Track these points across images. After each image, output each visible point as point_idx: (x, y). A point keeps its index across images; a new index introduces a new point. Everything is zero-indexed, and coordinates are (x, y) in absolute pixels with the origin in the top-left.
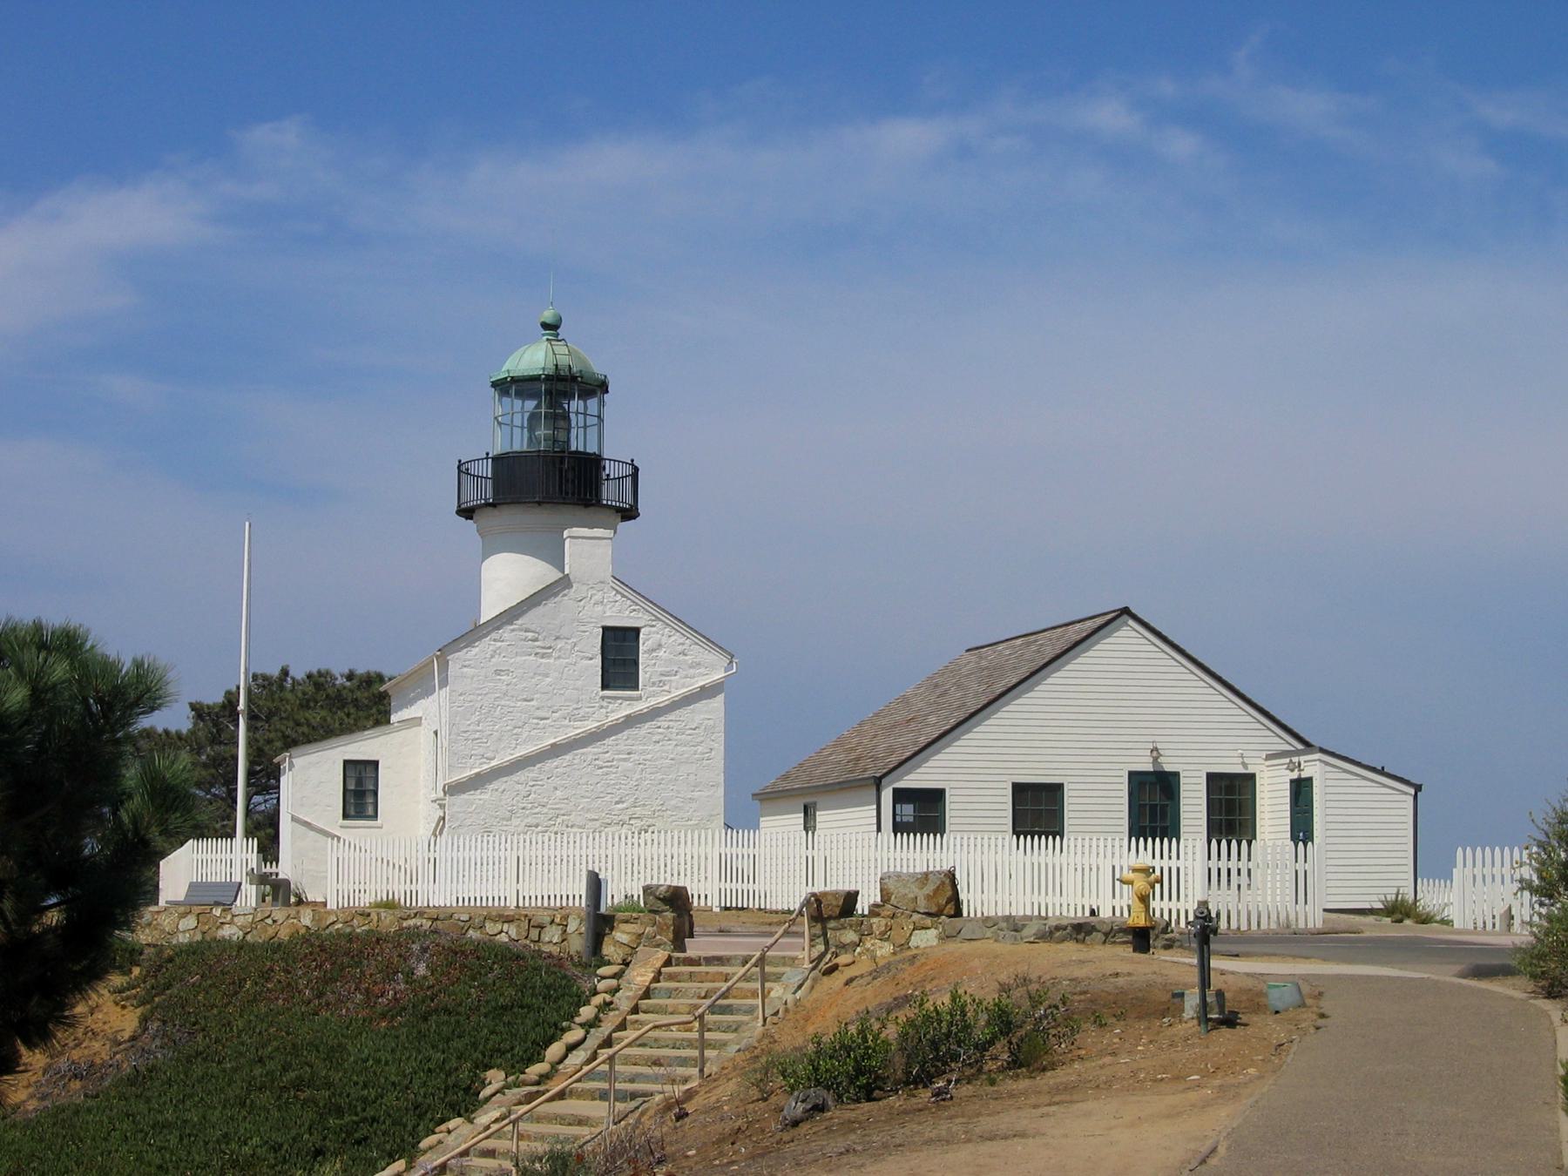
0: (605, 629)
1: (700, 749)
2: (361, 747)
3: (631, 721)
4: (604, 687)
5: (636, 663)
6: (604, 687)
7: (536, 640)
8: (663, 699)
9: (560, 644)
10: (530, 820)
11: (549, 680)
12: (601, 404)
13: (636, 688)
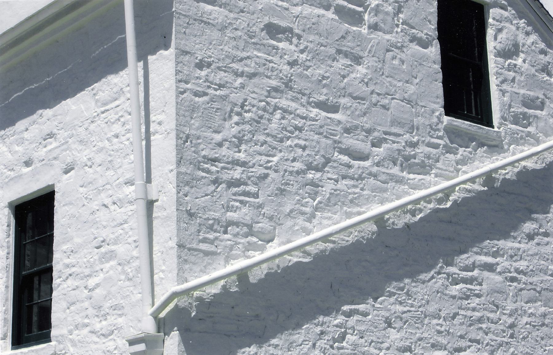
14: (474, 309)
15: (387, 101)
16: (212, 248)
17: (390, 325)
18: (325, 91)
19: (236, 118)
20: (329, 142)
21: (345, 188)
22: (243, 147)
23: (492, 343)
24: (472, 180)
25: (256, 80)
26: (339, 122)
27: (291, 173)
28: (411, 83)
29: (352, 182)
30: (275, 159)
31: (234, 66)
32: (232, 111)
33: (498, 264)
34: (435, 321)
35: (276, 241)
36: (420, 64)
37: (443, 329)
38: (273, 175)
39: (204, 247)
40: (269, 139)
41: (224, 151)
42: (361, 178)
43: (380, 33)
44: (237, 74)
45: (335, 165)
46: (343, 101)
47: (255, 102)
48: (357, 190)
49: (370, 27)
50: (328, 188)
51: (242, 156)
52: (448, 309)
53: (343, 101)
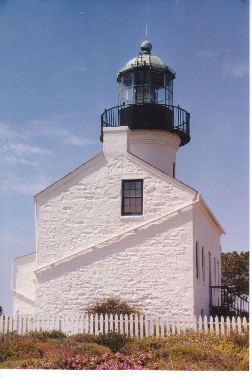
1: (178, 248)
9: (99, 190)
11: (92, 211)
14: (126, 267)
15: (99, 217)
16: (46, 261)
18: (79, 219)
20: (80, 232)
21: (84, 242)
22: (55, 238)
23: (133, 275)
24: (130, 232)
25: (59, 221)
27: (68, 241)
29: (86, 240)
30: (63, 239)
31: (54, 220)
32: (52, 230)
33: (137, 254)
34: (110, 271)
36: (112, 204)
38: (62, 242)
39: (43, 261)
41: (50, 239)
42: (89, 238)
44: (54, 221)
45: (81, 237)
46: (85, 220)
47: (59, 227)
48: (88, 242)
49: (95, 199)
50: (78, 242)
51: (54, 240)
52: (116, 267)
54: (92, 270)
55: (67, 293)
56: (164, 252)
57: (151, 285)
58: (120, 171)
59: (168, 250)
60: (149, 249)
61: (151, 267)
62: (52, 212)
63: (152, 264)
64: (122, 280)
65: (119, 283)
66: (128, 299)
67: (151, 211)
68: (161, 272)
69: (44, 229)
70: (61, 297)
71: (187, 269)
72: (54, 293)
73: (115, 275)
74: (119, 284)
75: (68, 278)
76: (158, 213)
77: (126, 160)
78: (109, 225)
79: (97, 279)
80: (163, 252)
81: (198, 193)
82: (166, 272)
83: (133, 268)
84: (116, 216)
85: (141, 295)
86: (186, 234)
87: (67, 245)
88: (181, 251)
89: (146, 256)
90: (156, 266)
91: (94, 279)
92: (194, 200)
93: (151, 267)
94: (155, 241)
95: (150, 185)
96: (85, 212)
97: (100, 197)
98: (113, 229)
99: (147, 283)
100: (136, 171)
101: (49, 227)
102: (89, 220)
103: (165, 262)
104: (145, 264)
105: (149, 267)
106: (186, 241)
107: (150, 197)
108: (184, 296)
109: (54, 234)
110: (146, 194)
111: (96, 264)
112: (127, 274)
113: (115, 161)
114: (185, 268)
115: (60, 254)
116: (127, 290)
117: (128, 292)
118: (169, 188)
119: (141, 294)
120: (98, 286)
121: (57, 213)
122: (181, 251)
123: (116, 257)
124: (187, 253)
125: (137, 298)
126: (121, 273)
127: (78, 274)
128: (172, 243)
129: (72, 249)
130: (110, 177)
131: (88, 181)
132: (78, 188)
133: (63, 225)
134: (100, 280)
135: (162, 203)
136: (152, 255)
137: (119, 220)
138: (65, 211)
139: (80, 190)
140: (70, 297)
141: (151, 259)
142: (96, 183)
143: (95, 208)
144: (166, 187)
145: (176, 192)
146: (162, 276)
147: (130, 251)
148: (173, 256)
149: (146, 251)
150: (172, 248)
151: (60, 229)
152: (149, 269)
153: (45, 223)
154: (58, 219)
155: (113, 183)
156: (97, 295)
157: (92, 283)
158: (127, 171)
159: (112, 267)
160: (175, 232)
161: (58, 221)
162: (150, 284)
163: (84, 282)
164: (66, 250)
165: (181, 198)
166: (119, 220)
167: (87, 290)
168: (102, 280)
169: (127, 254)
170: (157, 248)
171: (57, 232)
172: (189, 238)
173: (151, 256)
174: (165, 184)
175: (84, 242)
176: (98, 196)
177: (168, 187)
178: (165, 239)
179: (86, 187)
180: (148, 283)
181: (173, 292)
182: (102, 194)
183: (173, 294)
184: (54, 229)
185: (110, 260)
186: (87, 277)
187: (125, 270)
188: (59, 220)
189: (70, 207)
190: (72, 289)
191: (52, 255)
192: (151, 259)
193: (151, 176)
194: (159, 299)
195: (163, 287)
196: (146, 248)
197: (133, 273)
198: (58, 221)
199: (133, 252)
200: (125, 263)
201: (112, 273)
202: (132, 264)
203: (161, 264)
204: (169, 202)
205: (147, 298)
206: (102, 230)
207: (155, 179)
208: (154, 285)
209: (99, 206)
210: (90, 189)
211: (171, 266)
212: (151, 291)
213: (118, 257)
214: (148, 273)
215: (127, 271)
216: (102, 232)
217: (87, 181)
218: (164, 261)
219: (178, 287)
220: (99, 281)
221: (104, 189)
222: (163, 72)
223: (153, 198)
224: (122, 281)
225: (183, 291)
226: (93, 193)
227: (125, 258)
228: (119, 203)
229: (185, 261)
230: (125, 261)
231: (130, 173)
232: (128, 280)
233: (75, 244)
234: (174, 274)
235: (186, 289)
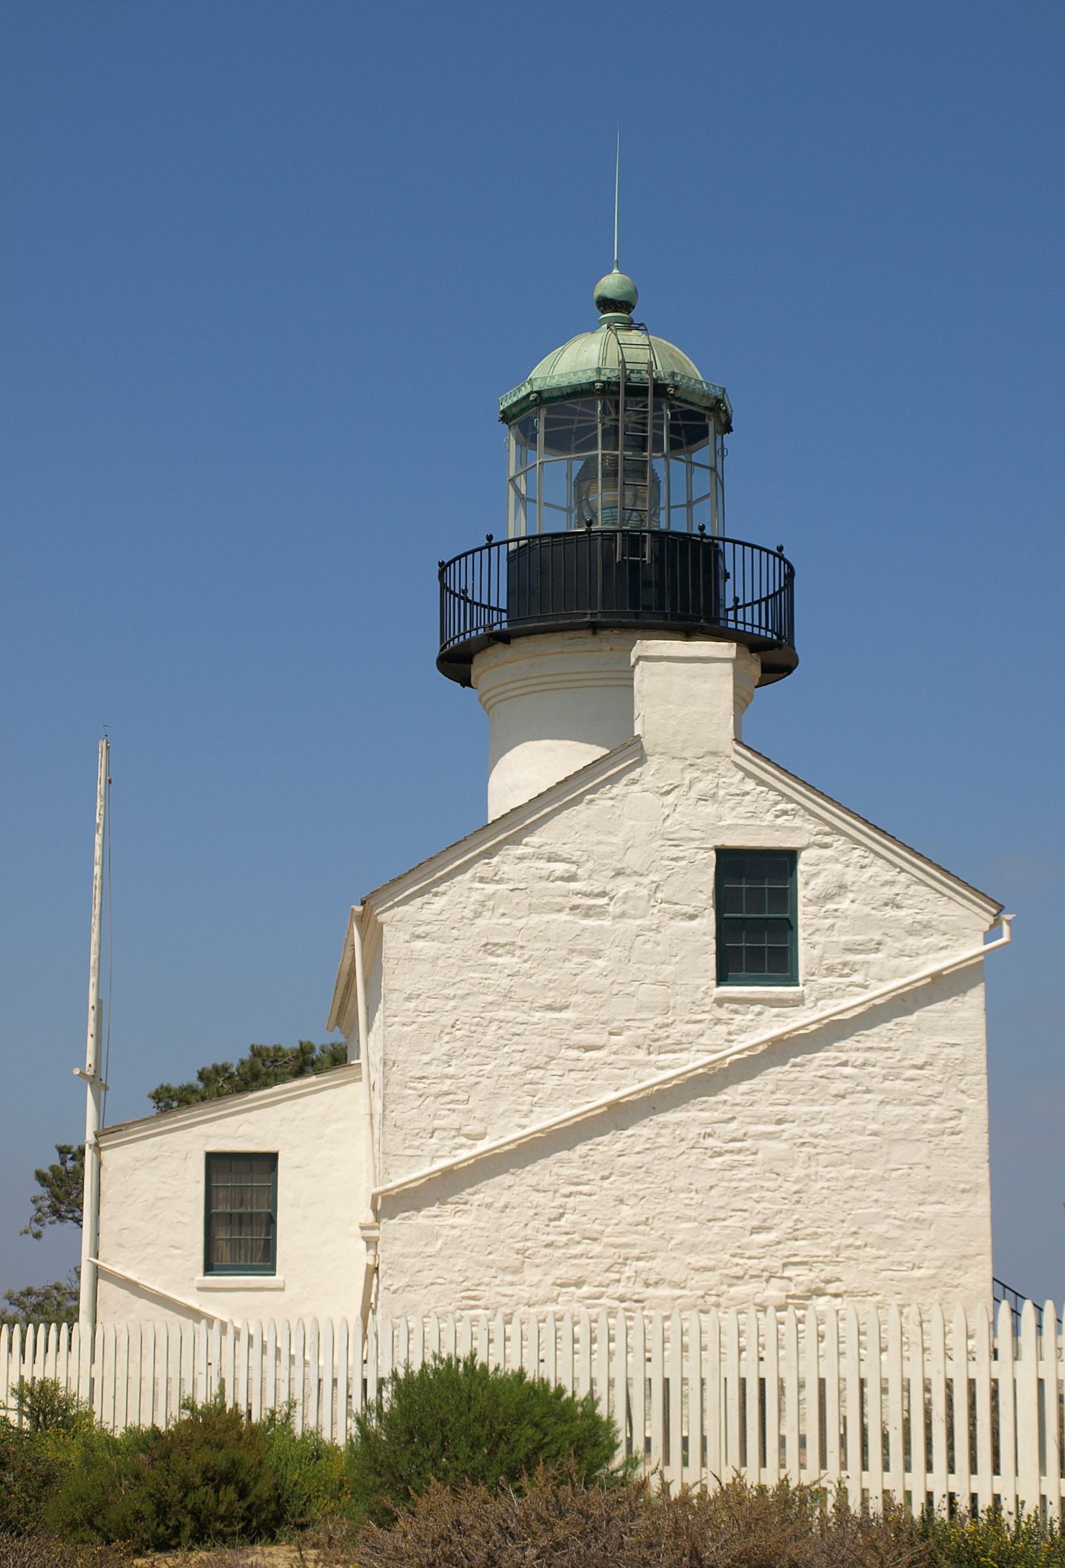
0: (722, 853)
1: (935, 1110)
2: (239, 1127)
3: (781, 1050)
4: (722, 978)
5: (788, 927)
6: (722, 978)
7: (572, 878)
8: (847, 1003)
9: (624, 886)
10: (563, 1272)
11: (601, 963)
12: (721, 453)
13: (793, 981)
14: (741, 1180)
15: (632, 989)
16: (419, 1152)
17: (622, 1201)
18: (552, 993)
19: (446, 1038)
20: (553, 1041)
21: (572, 1082)
22: (453, 1062)
23: (766, 1212)
25: (470, 999)
26: (568, 1021)
27: (506, 1077)
28: (669, 964)
30: (488, 1068)
31: (446, 992)
32: (442, 1031)
33: (783, 1131)
34: (683, 1195)
35: (487, 1138)
36: (683, 941)
37: (693, 1202)
38: (485, 1081)
39: (409, 1152)
40: (483, 1051)
41: (433, 1069)
42: (592, 1069)
43: (630, 921)
44: (447, 998)
45: (561, 1061)
46: (573, 999)
47: (468, 1020)
48: (589, 1081)
49: (614, 918)
51: (451, 1070)
52: (702, 1181)
53: (573, 999)
54: (607, 1189)
55: (509, 1278)
56: (883, 1123)
57: (838, 1248)
58: (709, 814)
59: (900, 1119)
60: (828, 1114)
61: (837, 1179)
62: (440, 963)
63: (838, 1168)
64: (726, 1227)
65: (717, 1239)
66: (750, 1298)
67: (830, 970)
68: (874, 1198)
69: (405, 1028)
70: (488, 1295)
71: (968, 1187)
72: (461, 1279)
73: (699, 1211)
74: (716, 1243)
75: (512, 1220)
76: (857, 978)
77: (730, 774)
78: (670, 1021)
79: (630, 1225)
80: (881, 1127)
81: (1001, 908)
82: (894, 1199)
83: (767, 1184)
84: (698, 988)
85: (801, 1284)
86: (962, 1062)
87: (503, 1091)
88: (944, 1120)
89: (815, 1141)
90: (854, 1178)
91: (617, 1224)
92: (988, 937)
93: (837, 1179)
94: (849, 1085)
95: (826, 873)
96: (572, 965)
97: (633, 912)
98: (688, 1035)
99: (820, 1241)
100: (769, 817)
101: (426, 1019)
102: (590, 998)
103: (887, 1161)
104: (812, 1170)
105: (828, 1180)
106: (962, 1086)
107: (826, 918)
108: (957, 1287)
109: (448, 1046)
110: (812, 909)
111: (625, 1170)
112: (745, 1207)
113: (689, 775)
114: (962, 1186)
115: (475, 1128)
116: (746, 1267)
117: (751, 1272)
118: (896, 889)
119: (801, 1278)
120: (635, 1252)
121: (460, 967)
122: (944, 1120)
123: (702, 1140)
124: (967, 1129)
125: (785, 1294)
126: (721, 1204)
127: (553, 1204)
128: (912, 1094)
129: (525, 1108)
130: (672, 836)
131: (584, 848)
132: (544, 873)
133: (488, 1015)
134: (641, 1228)
135: (872, 945)
136: (839, 1135)
137: (709, 1000)
138: (492, 959)
139: (552, 878)
140: (525, 1292)
141: (835, 1149)
142: (618, 858)
143: (616, 952)
144: (885, 883)
145: (922, 906)
146: (878, 1213)
147: (755, 1120)
148: (918, 1140)
149: (818, 1121)
150: (911, 1112)
151: (473, 1028)
152: (828, 1188)
153: (412, 1005)
154: (466, 992)
155: (683, 858)
156: (631, 1284)
157: (612, 1240)
158: (734, 813)
159: (688, 1181)
160: (922, 1052)
161: (463, 997)
162: (834, 1244)
163: (576, 1237)
164: (501, 1111)
165: (943, 927)
166: (712, 1000)
167: (590, 1268)
168: (648, 1228)
169: (742, 1131)
170: (858, 1109)
171: (461, 1039)
172: (975, 1074)
173: (835, 1139)
174: (879, 870)
175: (572, 1082)
176: (624, 907)
177: (892, 883)
178: (885, 1078)
179: (574, 868)
180: (827, 1238)
181: (917, 1273)
182: (639, 898)
183: (919, 1279)
184: (447, 1030)
185: (678, 1152)
186: (589, 1216)
187: (736, 1192)
188: (468, 994)
189: (513, 944)
190: (531, 1263)
191: (444, 1129)
192: (835, 1149)
193: (827, 839)
194: (868, 1298)
195: (882, 1253)
196: (817, 1108)
197: (769, 1201)
198: (463, 997)
199: (765, 1123)
200: (735, 1164)
201: (688, 1201)
202: (765, 1167)
203: (872, 1171)
204: (899, 940)
205: (819, 1293)
206: (645, 1036)
207: (844, 853)
208: (848, 1246)
209: (629, 945)
210: (590, 877)
211: (908, 1178)
212: (839, 1269)
213: (710, 1142)
214: (825, 1204)
215: (744, 1196)
216: (645, 1046)
217: (578, 847)
218: (884, 1159)
219: (938, 1253)
220: (636, 1233)
221: (646, 881)
222: (706, 408)
223: (839, 923)
224: (728, 1231)
225: (955, 1269)
226: (603, 894)
227: (738, 1145)
228: (707, 938)
229: (961, 1157)
230: (736, 1157)
231: (749, 822)
232: (749, 1228)
233: (537, 1091)
234: (920, 1204)
235: (965, 1262)
